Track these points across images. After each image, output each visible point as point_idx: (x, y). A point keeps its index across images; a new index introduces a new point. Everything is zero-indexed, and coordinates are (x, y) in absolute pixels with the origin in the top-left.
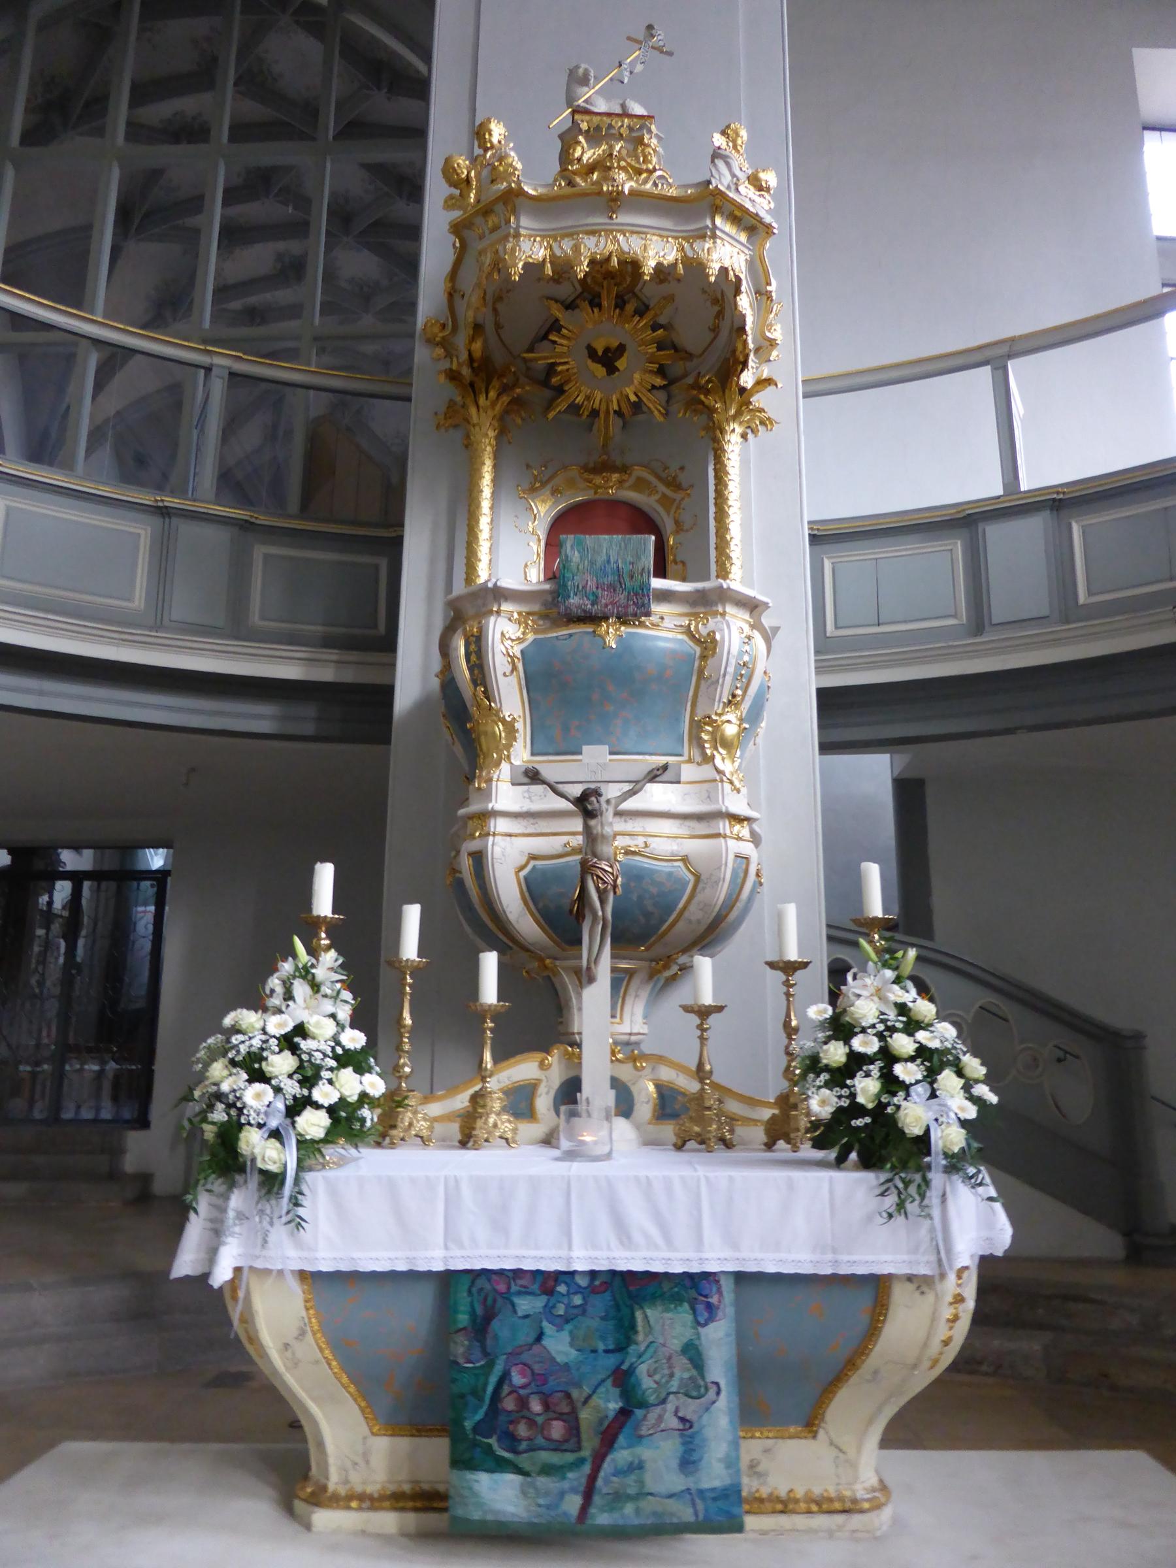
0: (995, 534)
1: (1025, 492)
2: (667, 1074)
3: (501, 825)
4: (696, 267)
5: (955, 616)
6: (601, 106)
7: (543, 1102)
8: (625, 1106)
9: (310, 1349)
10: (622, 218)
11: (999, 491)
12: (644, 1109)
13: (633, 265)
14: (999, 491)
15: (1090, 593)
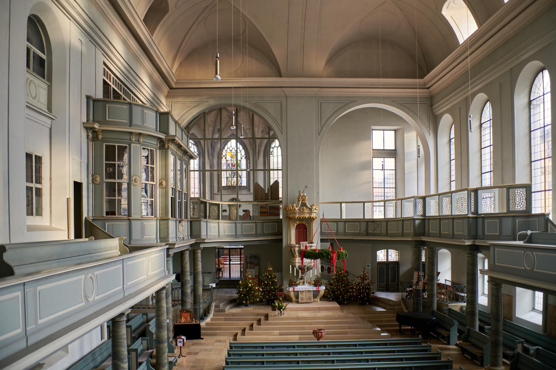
0: (339, 223)
1: (343, 219)
2: (309, 281)
3: (297, 263)
4: (311, 217)
5: (335, 231)
6: (302, 194)
7: (302, 283)
8: (307, 283)
9: (294, 295)
10: (305, 213)
11: (340, 218)
12: (308, 283)
13: (305, 217)
14: (340, 218)
15: (347, 231)
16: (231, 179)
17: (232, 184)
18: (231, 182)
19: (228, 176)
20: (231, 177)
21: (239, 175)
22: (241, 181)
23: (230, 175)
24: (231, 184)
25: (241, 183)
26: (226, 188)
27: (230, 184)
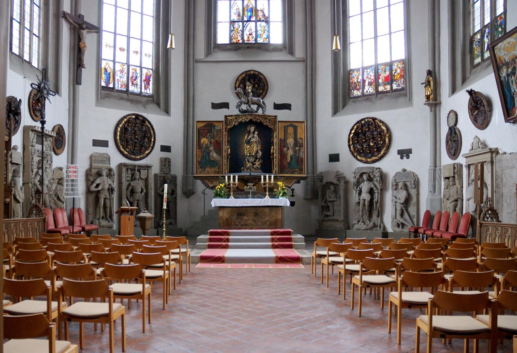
16: (243, 27)
17: (246, 38)
18: (243, 35)
19: (235, 17)
20: (243, 21)
21: (264, 15)
22: (269, 31)
23: (239, 15)
24: (243, 38)
25: (268, 37)
26: (229, 47)
27: (240, 38)
